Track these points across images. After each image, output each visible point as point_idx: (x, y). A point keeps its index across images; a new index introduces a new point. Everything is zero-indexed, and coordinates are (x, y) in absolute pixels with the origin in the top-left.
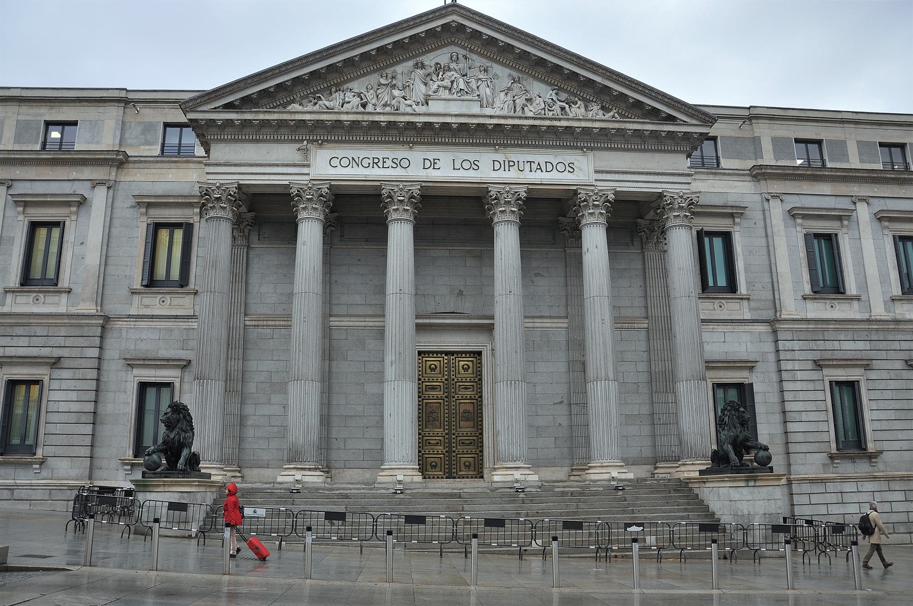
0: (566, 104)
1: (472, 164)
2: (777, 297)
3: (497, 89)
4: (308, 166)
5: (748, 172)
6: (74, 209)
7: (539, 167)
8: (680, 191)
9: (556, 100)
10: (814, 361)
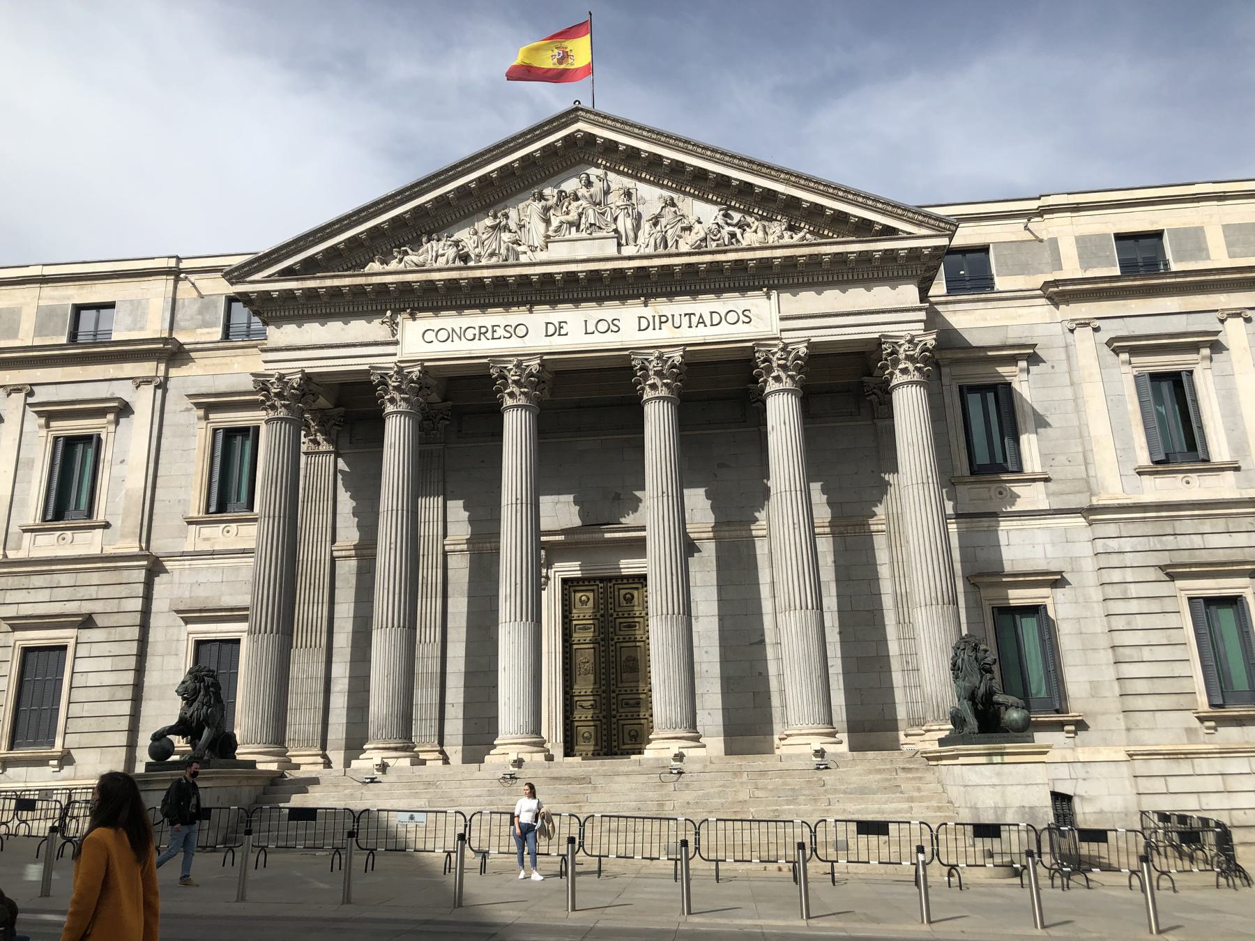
0: (739, 228)
1: (611, 325)
2: (1092, 473)
3: (645, 217)
4: (396, 343)
5: (1040, 292)
6: (111, 417)
7: (701, 321)
8: (907, 332)
9: (723, 225)
10: (1160, 567)
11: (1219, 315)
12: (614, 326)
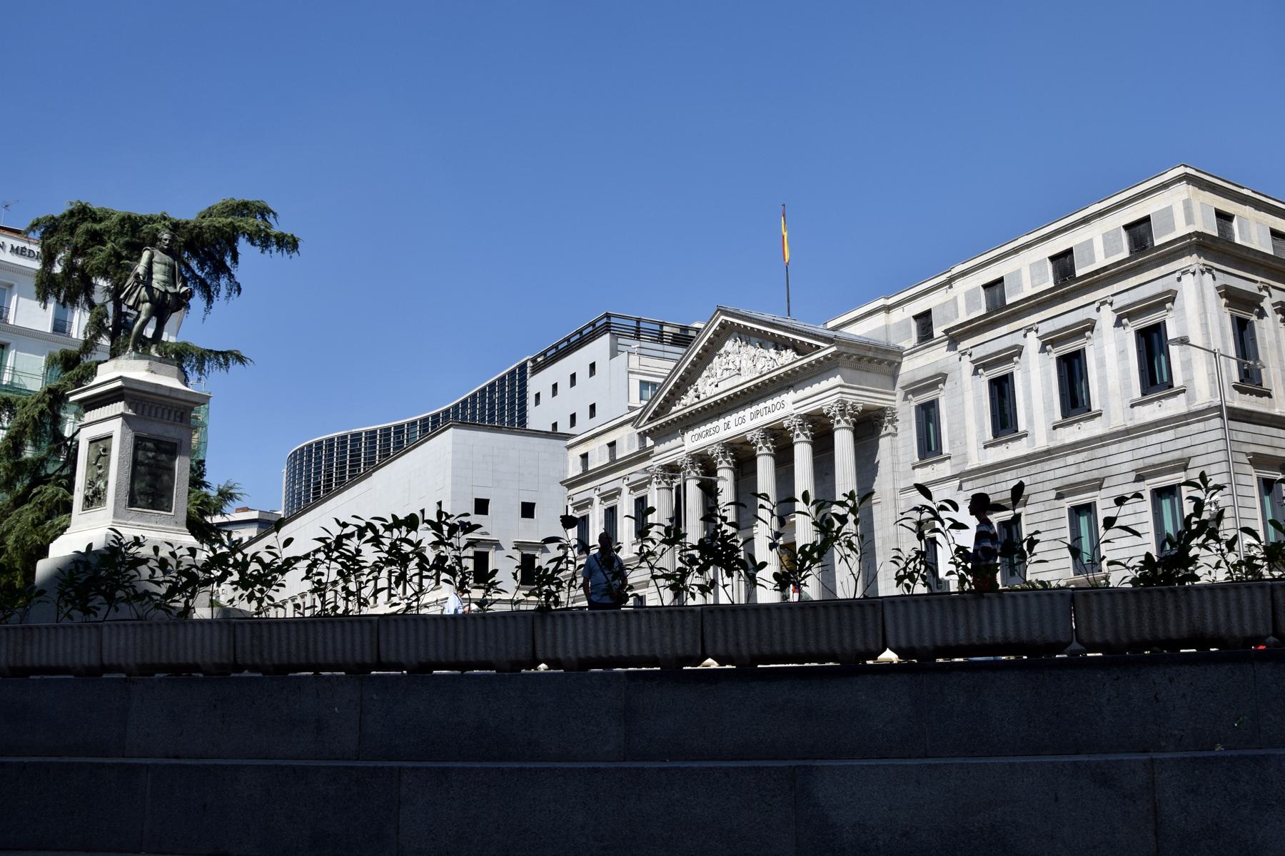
4: (683, 445)
11: (1023, 332)
12: (743, 421)
